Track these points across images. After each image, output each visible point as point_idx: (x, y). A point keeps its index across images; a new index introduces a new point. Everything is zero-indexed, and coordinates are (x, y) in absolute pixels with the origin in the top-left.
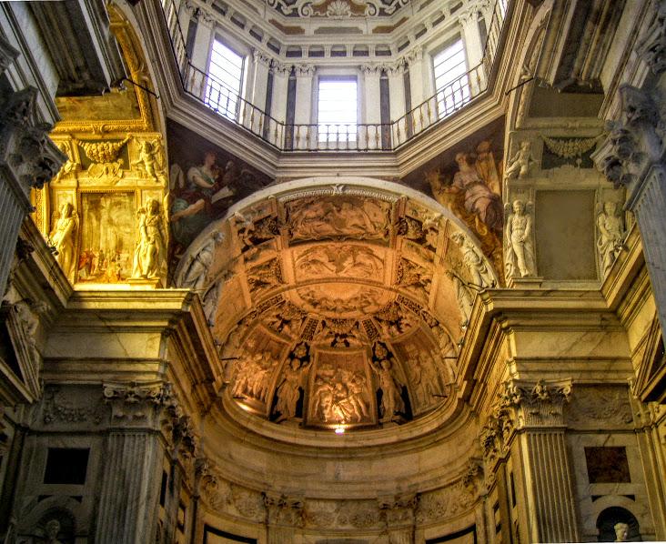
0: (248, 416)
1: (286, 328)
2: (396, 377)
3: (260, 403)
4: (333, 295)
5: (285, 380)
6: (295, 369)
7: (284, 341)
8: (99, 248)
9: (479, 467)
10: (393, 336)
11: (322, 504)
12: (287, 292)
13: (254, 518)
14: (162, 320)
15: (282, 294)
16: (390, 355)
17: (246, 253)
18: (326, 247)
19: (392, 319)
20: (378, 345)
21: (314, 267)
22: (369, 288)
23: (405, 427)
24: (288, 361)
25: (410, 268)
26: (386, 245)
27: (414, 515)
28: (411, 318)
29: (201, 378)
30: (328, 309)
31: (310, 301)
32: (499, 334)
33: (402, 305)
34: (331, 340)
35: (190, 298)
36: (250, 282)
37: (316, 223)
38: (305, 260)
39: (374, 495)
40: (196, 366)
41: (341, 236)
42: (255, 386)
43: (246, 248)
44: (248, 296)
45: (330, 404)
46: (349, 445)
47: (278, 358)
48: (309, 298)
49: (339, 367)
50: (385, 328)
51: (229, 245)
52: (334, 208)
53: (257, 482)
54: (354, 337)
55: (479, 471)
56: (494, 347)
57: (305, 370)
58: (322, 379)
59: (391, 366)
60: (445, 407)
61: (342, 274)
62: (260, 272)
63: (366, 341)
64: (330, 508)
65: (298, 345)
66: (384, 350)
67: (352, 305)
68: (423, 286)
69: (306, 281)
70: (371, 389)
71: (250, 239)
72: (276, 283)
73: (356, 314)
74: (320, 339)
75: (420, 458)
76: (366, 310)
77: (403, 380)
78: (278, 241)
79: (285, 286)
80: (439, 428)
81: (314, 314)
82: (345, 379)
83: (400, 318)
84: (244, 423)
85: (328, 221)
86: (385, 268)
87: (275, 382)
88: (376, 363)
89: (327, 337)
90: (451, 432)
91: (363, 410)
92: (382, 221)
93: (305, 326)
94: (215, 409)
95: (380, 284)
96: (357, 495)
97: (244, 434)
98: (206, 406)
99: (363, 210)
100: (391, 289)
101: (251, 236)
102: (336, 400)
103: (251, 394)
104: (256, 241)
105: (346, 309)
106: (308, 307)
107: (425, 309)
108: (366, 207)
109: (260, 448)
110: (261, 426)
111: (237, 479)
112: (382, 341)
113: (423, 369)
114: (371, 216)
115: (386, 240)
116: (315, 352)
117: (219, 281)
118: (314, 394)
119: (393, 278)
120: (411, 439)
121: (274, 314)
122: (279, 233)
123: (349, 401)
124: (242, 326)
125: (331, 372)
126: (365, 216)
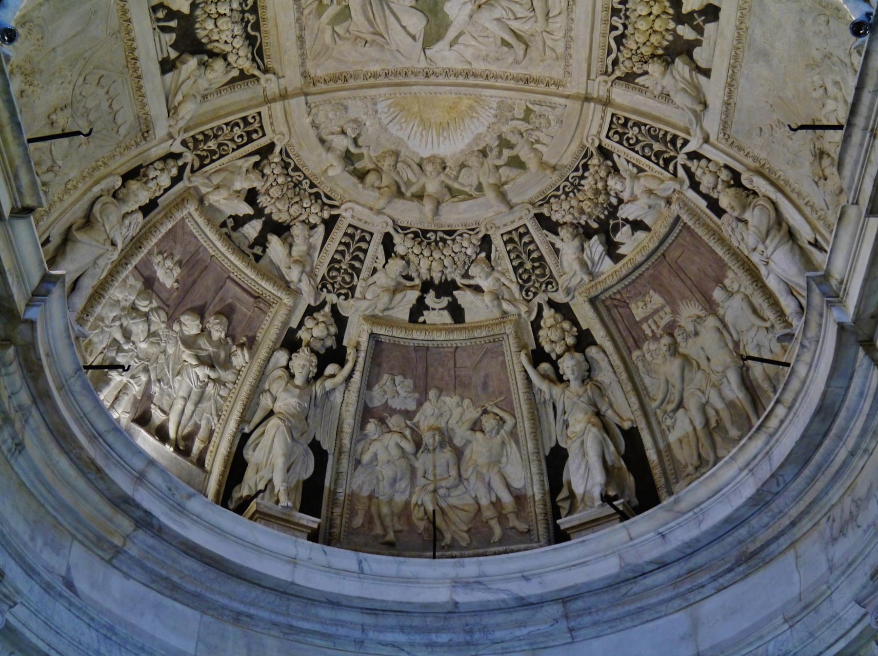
0: (139, 464)
1: (275, 243)
2: (604, 408)
6: (299, 380)
10: (590, 274)
12: (278, 107)
16: (584, 341)
20: (547, 312)
23: (644, 524)
24: (281, 357)
30: (400, 194)
34: (412, 296)
42: (179, 405)
44: (154, 82)
46: (463, 597)
47: (251, 344)
48: (342, 143)
50: (568, 245)
54: (477, 289)
58: (382, 421)
59: (588, 375)
60: (781, 411)
61: (443, 55)
65: (310, 311)
66: (566, 325)
67: (467, 181)
69: (335, 79)
70: (531, 445)
72: (246, 64)
74: (374, 301)
75: (695, 625)
77: (624, 409)
79: (269, 84)
80: (760, 501)
81: (361, 208)
83: (613, 210)
84: (123, 482)
88: (545, 366)
89: (395, 291)
90: (794, 512)
93: (333, 245)
100: (587, 99)
103: (161, 433)
107: (689, 148)
109: (172, 589)
110: (180, 509)
112: (560, 297)
113: (686, 359)
116: (357, 333)
119: (597, 52)
120: (662, 565)
121: (242, 184)
124: (134, 185)
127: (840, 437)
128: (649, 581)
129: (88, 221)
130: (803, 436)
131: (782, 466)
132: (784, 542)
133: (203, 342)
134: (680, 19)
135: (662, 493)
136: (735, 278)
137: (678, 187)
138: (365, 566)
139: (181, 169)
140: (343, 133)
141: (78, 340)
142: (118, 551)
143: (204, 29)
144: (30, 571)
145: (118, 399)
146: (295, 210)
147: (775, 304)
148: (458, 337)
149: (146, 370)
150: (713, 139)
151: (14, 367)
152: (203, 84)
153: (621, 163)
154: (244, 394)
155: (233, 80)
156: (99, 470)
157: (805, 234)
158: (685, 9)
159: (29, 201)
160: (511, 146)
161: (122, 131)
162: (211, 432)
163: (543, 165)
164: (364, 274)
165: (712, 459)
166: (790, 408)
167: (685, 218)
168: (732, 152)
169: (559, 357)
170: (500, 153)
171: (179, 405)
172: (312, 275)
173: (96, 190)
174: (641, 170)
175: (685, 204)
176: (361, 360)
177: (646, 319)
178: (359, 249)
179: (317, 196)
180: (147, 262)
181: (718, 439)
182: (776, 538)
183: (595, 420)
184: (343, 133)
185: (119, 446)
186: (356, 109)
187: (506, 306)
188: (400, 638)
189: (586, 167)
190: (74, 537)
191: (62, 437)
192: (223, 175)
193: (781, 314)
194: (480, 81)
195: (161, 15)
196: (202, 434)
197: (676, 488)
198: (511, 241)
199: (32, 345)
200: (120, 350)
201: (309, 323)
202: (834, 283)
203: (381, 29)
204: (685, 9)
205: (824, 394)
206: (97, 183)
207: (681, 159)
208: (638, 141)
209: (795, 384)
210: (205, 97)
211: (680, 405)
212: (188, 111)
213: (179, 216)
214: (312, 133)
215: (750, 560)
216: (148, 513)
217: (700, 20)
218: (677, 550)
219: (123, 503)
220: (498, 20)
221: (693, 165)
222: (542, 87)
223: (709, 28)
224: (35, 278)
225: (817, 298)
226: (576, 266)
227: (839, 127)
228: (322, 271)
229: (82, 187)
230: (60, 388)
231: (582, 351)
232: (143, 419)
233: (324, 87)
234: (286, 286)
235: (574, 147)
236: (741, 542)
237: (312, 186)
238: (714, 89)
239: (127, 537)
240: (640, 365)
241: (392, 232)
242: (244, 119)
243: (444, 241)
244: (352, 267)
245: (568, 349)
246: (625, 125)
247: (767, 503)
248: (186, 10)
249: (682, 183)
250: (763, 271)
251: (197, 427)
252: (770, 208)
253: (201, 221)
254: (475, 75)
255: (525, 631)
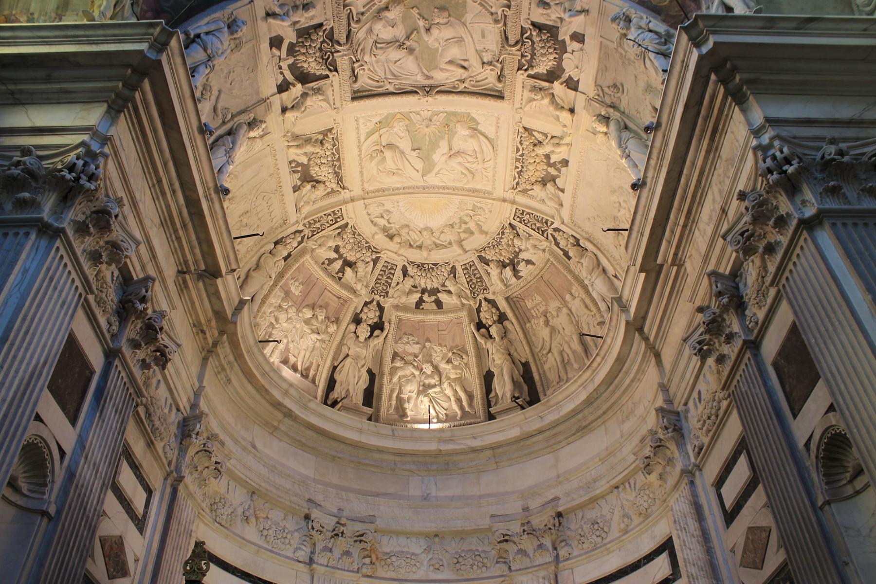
0: (285, 386)
3: (307, 383)
4: (419, 222)
5: (348, 355)
6: (362, 339)
7: (345, 293)
8: (28, 10)
9: (675, 425)
11: (403, 540)
12: (350, 205)
13: (290, 554)
14: (110, 79)
15: (343, 207)
17: (285, 95)
18: (406, 116)
19: (506, 256)
20: (483, 303)
21: (388, 154)
22: (470, 201)
23: (531, 411)
24: (352, 327)
25: (535, 145)
26: (499, 96)
27: (555, 549)
28: (535, 247)
29: (196, 262)
31: (384, 230)
32: (721, 111)
33: (521, 227)
34: (417, 296)
35: (163, 39)
36: (295, 166)
37: (394, 54)
38: (377, 143)
39: (486, 523)
40: (184, 226)
41: (432, 87)
42: (302, 354)
43: (283, 87)
44: (290, 197)
45: (414, 395)
46: (445, 447)
47: (337, 321)
48: (382, 222)
49: (428, 340)
50: (494, 271)
51: (256, 65)
52: (421, 23)
53: (297, 495)
54: (449, 292)
55: (674, 430)
56: (708, 152)
57: (377, 342)
58: (403, 359)
59: (505, 334)
60: (598, 359)
62: (309, 149)
63: (467, 298)
64: (416, 547)
65: (366, 304)
66: (494, 310)
68: (553, 179)
69: (378, 191)
71: (289, 66)
72: (334, 186)
73: (453, 255)
76: (467, 245)
78: (337, 85)
79: (346, 195)
80: (589, 402)
81: (393, 253)
82: (437, 359)
83: (517, 255)
84: (277, 395)
85: (411, 51)
86: (496, 156)
87: (332, 353)
88: (483, 330)
89: (409, 293)
90: (605, 407)
91: (465, 403)
92: (495, 49)
93: (377, 271)
94: (224, 351)
95: (486, 194)
96: (459, 525)
97: (277, 415)
98: (210, 341)
99: (464, 24)
100: (504, 201)
101: (291, 61)
102: (424, 389)
103: (294, 368)
104: (304, 78)
105: (437, 246)
106: (380, 241)
107: (554, 226)
108: (469, 17)
109: (303, 446)
110: (305, 407)
111: (263, 484)
113: (553, 330)
114: (477, 37)
115: (500, 86)
116: (391, 315)
117: (239, 126)
118: (391, 379)
119: (509, 178)
120: (541, 432)
121: (332, 244)
122: (336, 70)
123: (442, 391)
125: (416, 349)
126: (468, 39)
127: (627, 373)
128: (534, 439)
129: (258, 266)
130: (609, 372)
131: (599, 386)
132: (600, 421)
133: (314, 322)
134: (549, 165)
135: (541, 395)
136: (576, 289)
137: (548, 244)
138: (396, 433)
139: (303, 238)
140: (382, 217)
141: (255, 326)
142: (276, 428)
143: (314, 171)
144: (236, 441)
145: (273, 354)
146: (358, 255)
147: (596, 304)
148: (440, 318)
149: (286, 337)
150: (566, 221)
151: (227, 344)
152: (313, 197)
153: (521, 232)
154: (334, 347)
155: (328, 193)
156: (266, 390)
157: (611, 271)
158: (552, 161)
159: (234, 267)
160: (466, 223)
161: (274, 221)
162: (318, 366)
163: (482, 232)
164: (393, 285)
165: (565, 379)
166: (603, 358)
167: (552, 260)
168: (576, 228)
169: (490, 326)
170: (460, 227)
171: (302, 354)
172: (367, 287)
173: (262, 251)
174: (530, 236)
175: (552, 253)
176: (392, 329)
177: (533, 308)
178: (391, 273)
179: (369, 248)
180: (286, 284)
181: (568, 368)
182: (596, 419)
183: (508, 357)
184: (382, 217)
185: (276, 378)
186: (388, 206)
187: (465, 301)
188: (413, 467)
189: (503, 233)
190: (255, 423)
191: (249, 375)
192: (323, 239)
193: (599, 310)
194: (450, 191)
195: (293, 165)
196: (314, 367)
197: (548, 393)
198: (466, 269)
199: (236, 334)
200: (274, 327)
201: (366, 310)
202: (624, 300)
203: (401, 167)
204: (552, 161)
205: (619, 353)
206: (262, 247)
207: (550, 231)
208: (529, 222)
209: (606, 347)
210: (314, 202)
211: (550, 351)
212: (306, 210)
213: (302, 261)
214: (367, 218)
215: (583, 430)
216: (290, 410)
217: (559, 166)
218: (548, 424)
219: (278, 405)
220: (459, 163)
221: (556, 234)
222: (481, 195)
223: (563, 170)
224: (237, 302)
225: (616, 307)
226: (499, 282)
227: (626, 230)
228: (372, 284)
229: (255, 249)
230: (248, 352)
231: (502, 323)
232: (285, 362)
233: (373, 195)
234: (354, 292)
235: (497, 224)
236: (579, 421)
237: (367, 242)
238: (566, 198)
239: (280, 421)
240: (530, 330)
241: (407, 265)
242: (333, 212)
243: (433, 269)
244: (387, 282)
245: (495, 322)
246: (522, 214)
247: (592, 403)
248: (306, 163)
249: (551, 243)
250: (590, 289)
251: (312, 363)
252: (594, 257)
253: (312, 262)
254: (448, 188)
255: (474, 463)
